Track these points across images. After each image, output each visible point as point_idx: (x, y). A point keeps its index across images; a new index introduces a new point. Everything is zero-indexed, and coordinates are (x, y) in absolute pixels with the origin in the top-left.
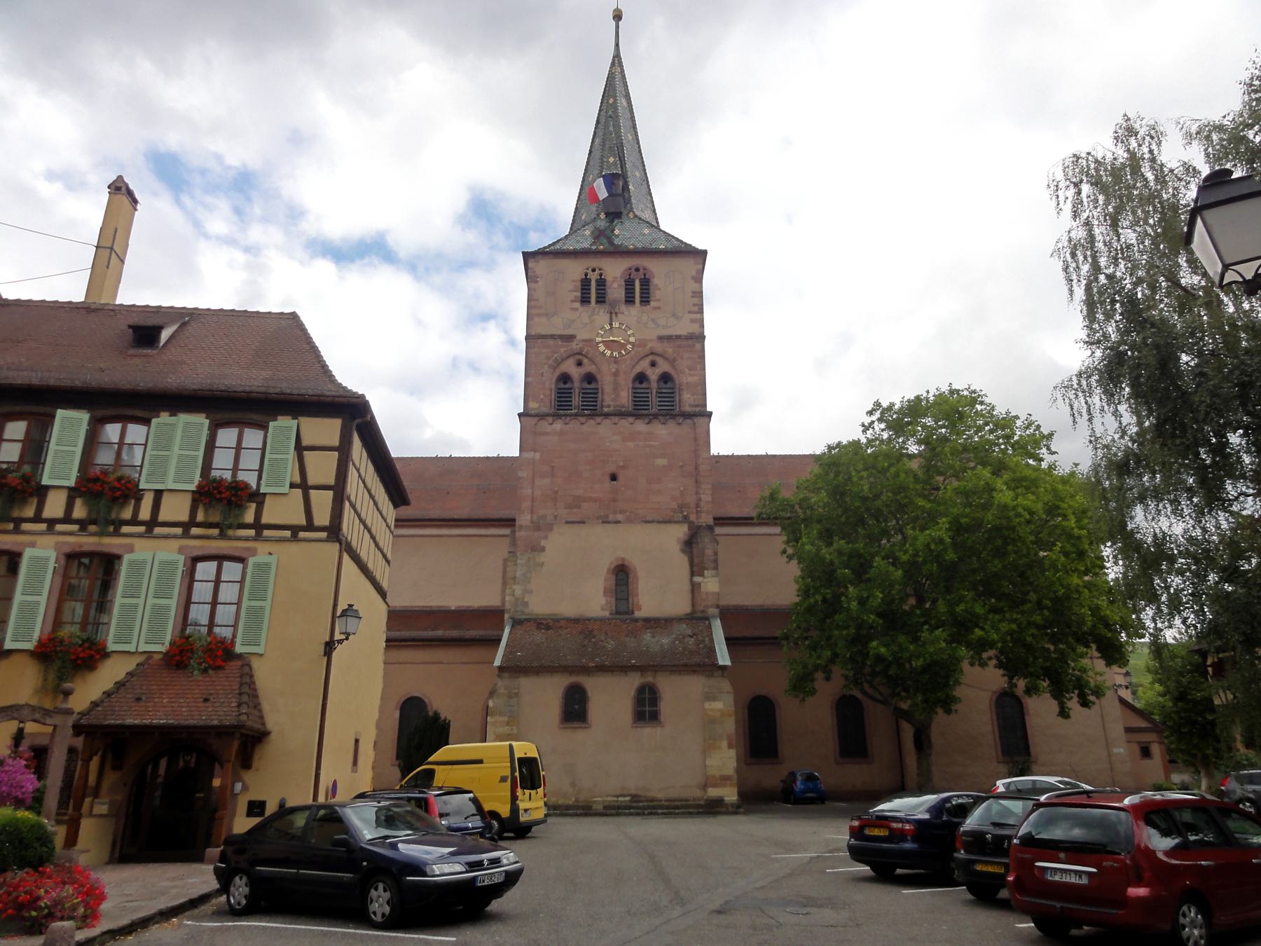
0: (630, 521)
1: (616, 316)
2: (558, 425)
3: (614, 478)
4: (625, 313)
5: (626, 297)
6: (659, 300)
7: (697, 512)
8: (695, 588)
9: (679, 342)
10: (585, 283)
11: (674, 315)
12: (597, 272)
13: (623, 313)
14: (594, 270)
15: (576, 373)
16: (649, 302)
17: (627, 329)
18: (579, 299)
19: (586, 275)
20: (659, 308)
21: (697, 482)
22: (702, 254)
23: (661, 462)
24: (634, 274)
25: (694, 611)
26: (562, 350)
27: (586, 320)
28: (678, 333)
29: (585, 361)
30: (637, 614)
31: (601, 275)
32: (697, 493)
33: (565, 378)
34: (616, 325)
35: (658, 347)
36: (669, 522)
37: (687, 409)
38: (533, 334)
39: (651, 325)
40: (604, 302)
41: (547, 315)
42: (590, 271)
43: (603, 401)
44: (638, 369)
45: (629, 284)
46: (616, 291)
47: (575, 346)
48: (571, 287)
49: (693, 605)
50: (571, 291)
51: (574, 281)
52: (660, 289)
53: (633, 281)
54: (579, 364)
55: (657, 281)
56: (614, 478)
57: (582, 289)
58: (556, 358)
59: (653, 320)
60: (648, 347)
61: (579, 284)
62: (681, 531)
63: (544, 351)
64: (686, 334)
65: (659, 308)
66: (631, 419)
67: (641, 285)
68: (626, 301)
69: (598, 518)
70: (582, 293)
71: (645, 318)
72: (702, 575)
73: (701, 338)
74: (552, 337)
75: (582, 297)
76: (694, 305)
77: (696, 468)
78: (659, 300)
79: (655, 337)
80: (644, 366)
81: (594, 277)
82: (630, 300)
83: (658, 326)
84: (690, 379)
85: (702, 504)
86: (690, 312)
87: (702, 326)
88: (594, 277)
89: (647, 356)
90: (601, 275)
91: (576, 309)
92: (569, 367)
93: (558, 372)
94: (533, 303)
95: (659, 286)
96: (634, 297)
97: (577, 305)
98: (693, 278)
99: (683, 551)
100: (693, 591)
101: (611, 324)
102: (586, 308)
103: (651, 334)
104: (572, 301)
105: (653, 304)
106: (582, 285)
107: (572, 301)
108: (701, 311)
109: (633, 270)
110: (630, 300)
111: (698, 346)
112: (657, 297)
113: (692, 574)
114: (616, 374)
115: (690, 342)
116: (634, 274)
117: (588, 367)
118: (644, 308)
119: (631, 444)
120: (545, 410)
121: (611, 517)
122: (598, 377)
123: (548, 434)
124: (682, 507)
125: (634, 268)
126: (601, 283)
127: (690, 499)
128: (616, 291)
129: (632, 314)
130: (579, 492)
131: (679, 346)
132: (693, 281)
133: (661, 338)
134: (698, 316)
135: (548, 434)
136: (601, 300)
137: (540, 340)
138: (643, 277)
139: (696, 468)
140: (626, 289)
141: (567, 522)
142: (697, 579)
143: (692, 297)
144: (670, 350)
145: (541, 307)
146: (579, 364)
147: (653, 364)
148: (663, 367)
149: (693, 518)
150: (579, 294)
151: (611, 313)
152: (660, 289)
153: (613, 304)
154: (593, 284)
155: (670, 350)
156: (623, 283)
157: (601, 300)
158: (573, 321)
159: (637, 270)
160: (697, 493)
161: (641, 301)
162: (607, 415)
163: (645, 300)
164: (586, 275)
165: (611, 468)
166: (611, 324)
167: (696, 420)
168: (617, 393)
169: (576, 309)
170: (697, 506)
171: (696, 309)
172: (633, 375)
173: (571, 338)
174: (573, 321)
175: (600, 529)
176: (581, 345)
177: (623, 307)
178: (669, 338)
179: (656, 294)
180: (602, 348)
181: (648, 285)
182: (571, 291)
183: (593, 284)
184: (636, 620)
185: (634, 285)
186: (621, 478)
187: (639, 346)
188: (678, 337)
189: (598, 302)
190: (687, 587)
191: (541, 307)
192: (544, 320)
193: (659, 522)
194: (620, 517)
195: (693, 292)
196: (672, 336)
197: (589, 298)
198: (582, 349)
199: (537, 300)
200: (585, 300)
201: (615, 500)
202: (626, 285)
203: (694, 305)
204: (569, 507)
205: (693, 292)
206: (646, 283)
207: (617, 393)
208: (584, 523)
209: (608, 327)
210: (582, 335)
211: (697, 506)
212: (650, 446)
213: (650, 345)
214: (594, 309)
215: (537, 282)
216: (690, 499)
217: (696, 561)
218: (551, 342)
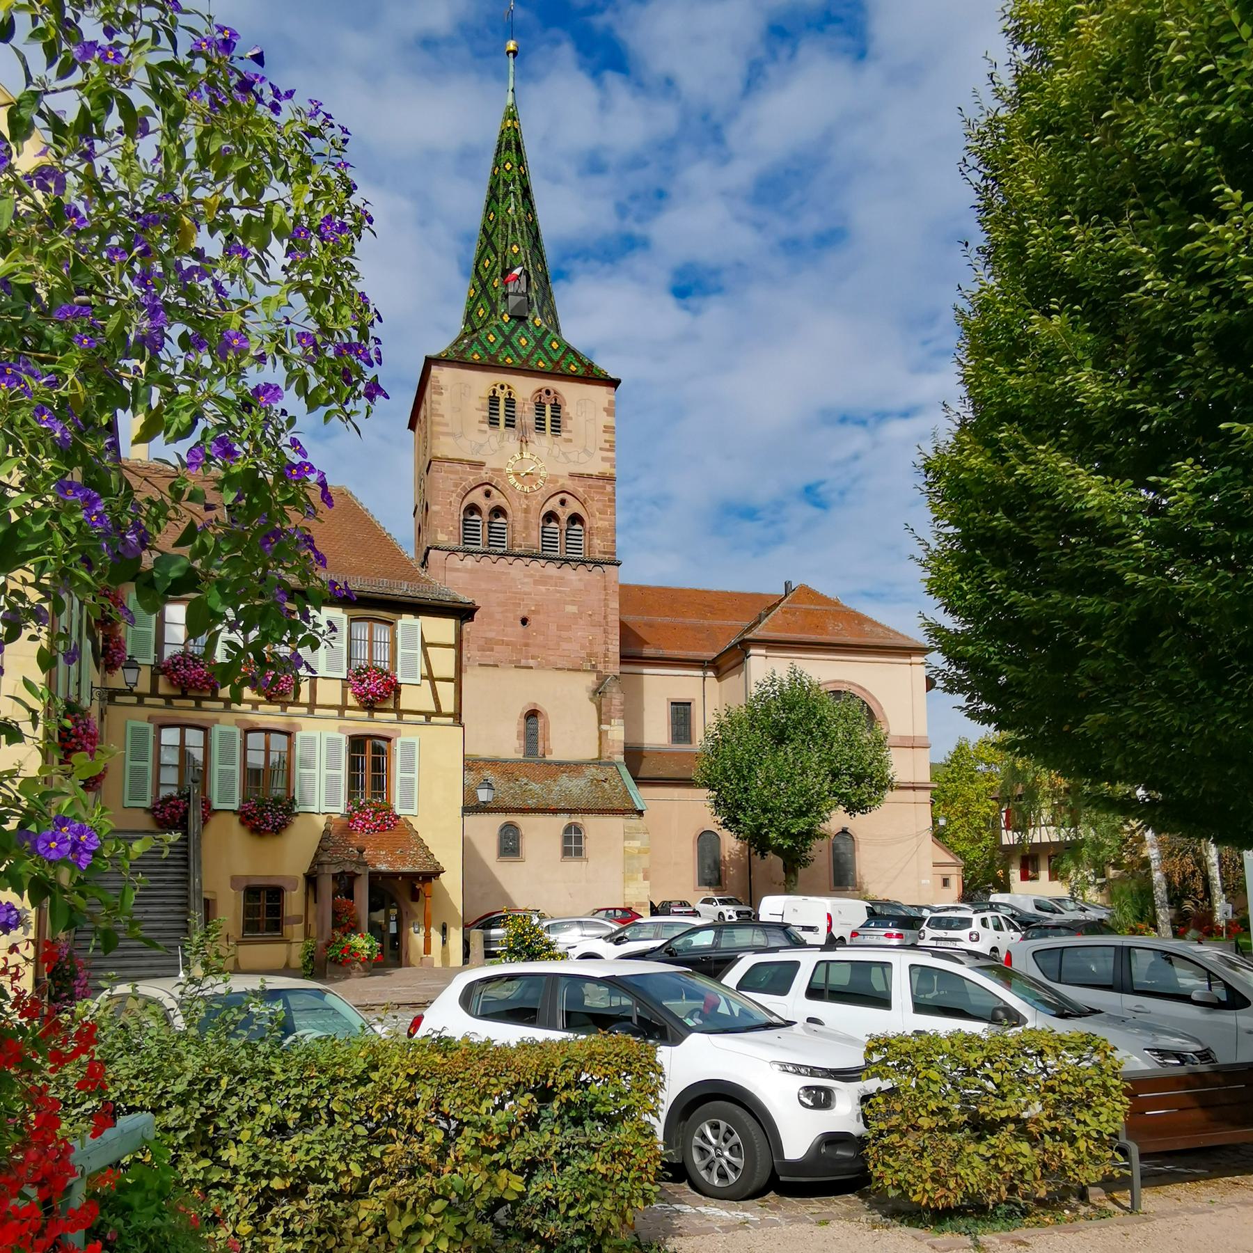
0: (541, 667)
2: (470, 561)
3: (524, 621)
6: (570, 432)
7: (605, 662)
8: (602, 735)
9: (590, 482)
10: (494, 400)
11: (585, 450)
14: (502, 387)
15: (485, 505)
18: (487, 420)
19: (494, 392)
20: (570, 441)
21: (605, 632)
23: (572, 609)
24: (545, 399)
25: (600, 757)
27: (496, 446)
29: (494, 492)
30: (548, 758)
31: (510, 394)
32: (606, 643)
33: (473, 509)
34: (526, 455)
35: (570, 485)
36: (579, 670)
37: (598, 556)
39: (562, 459)
42: (498, 388)
43: (513, 539)
44: (547, 508)
45: (540, 407)
46: (526, 414)
47: (484, 475)
48: (478, 404)
49: (600, 752)
54: (488, 494)
55: (569, 409)
56: (524, 621)
59: (564, 454)
61: (487, 402)
62: (590, 680)
63: (452, 476)
65: (570, 441)
66: (543, 562)
69: (511, 662)
71: (556, 451)
72: (609, 724)
74: (460, 461)
77: (605, 617)
78: (570, 432)
80: (553, 504)
81: (501, 395)
82: (540, 427)
84: (600, 524)
85: (610, 654)
90: (510, 394)
91: (485, 432)
92: (477, 497)
93: (465, 504)
97: (486, 427)
98: (605, 410)
99: (591, 700)
100: (600, 738)
102: (495, 432)
103: (563, 470)
105: (564, 435)
110: (540, 427)
113: (600, 722)
114: (527, 511)
115: (601, 483)
117: (498, 499)
119: (543, 588)
120: (454, 544)
121: (523, 662)
122: (509, 512)
123: (457, 570)
124: (590, 655)
126: (510, 402)
127: (600, 649)
128: (526, 414)
129: (542, 443)
130: (491, 635)
131: (590, 486)
133: (572, 475)
135: (457, 570)
139: (605, 617)
141: (481, 665)
142: (604, 727)
144: (581, 490)
145: (446, 425)
146: (488, 494)
147: (563, 502)
148: (574, 507)
149: (600, 667)
150: (487, 414)
153: (524, 428)
154: (502, 403)
155: (581, 490)
157: (510, 423)
158: (481, 446)
159: (548, 392)
160: (606, 643)
162: (519, 556)
163: (557, 427)
164: (494, 392)
165: (523, 613)
167: (605, 567)
168: (526, 533)
169: (485, 432)
170: (606, 656)
171: (607, 446)
172: (542, 514)
175: (515, 673)
177: (533, 436)
178: (581, 476)
179: (568, 425)
180: (512, 480)
183: (502, 403)
184: (549, 763)
186: (532, 622)
187: (550, 482)
188: (590, 476)
190: (597, 734)
191: (446, 425)
192: (450, 440)
193: (569, 670)
194: (531, 662)
200: (493, 422)
201: (527, 645)
204: (481, 649)
206: (556, 408)
207: (526, 533)
208: (497, 666)
209: (518, 457)
210: (492, 463)
211: (606, 656)
212: (560, 592)
213: (561, 481)
216: (600, 649)
217: (604, 709)
218: (458, 467)
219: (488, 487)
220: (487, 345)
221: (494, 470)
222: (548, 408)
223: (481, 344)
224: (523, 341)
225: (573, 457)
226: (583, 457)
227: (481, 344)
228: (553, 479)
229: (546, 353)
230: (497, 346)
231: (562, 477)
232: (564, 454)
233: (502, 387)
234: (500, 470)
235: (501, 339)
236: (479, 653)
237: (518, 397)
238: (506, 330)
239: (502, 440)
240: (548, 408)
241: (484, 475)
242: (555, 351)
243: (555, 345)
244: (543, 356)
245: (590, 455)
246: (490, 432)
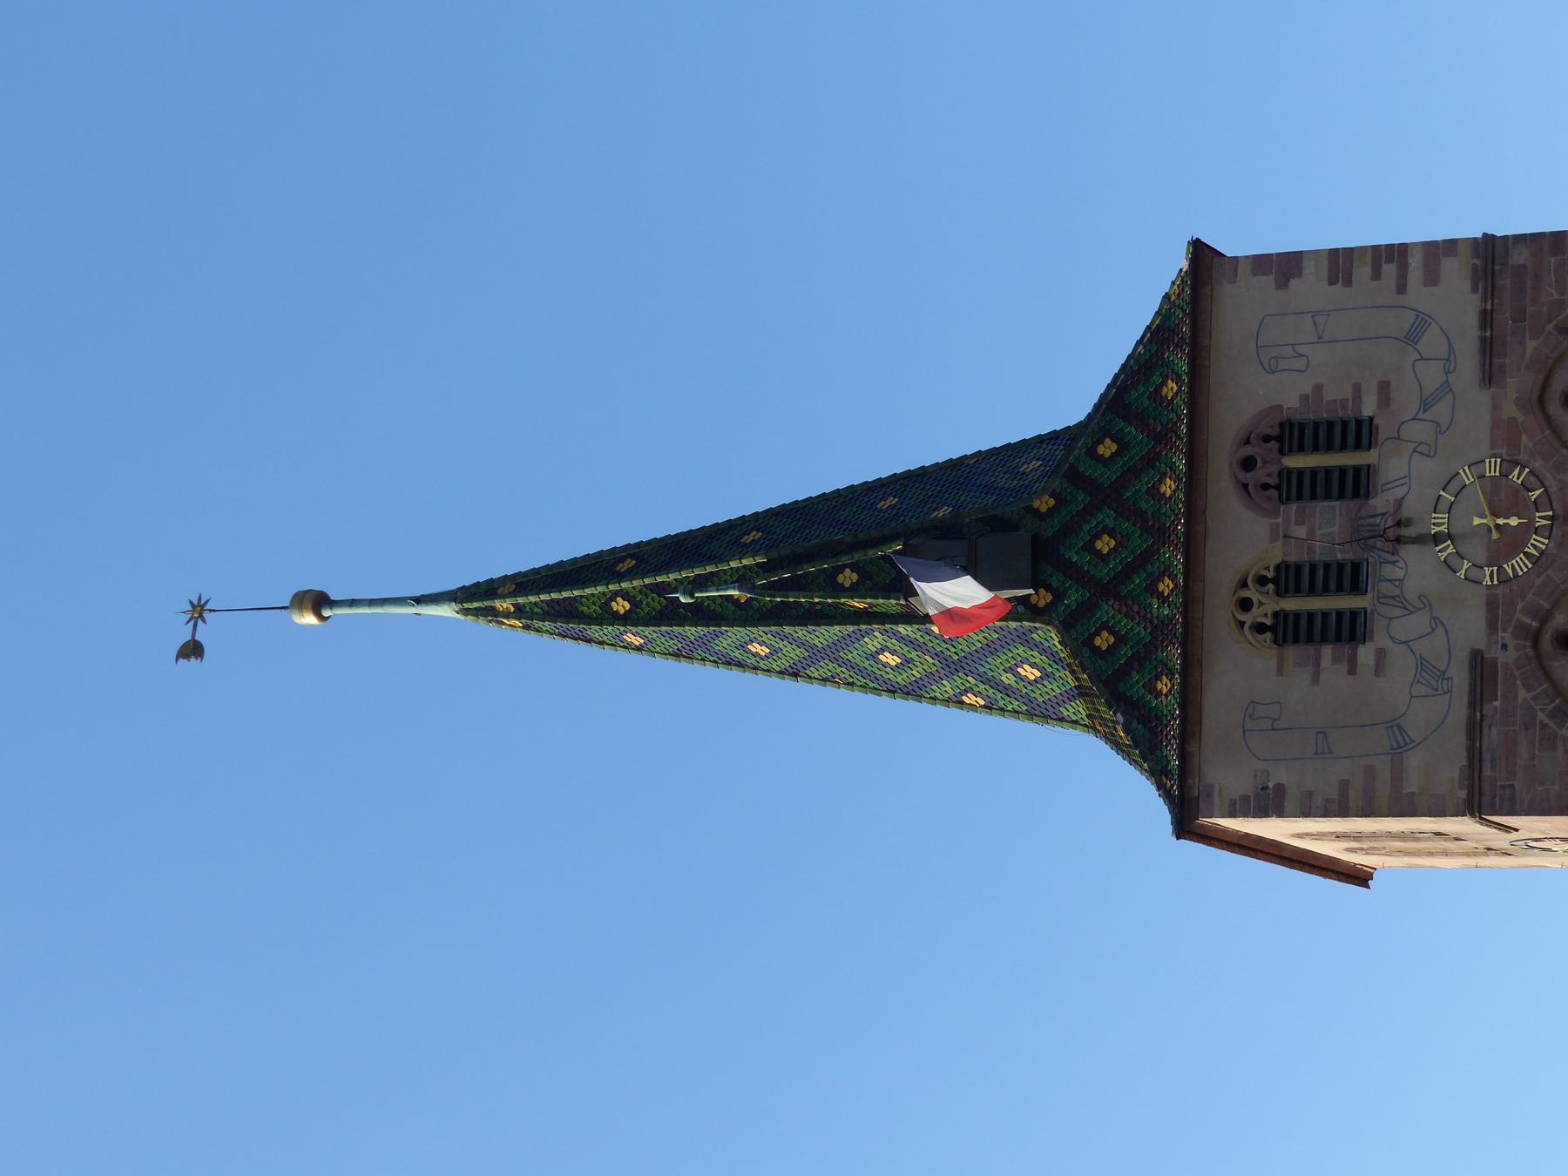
1: (1409, 522)
4: (1399, 492)
5: (1341, 496)
6: (1357, 389)
11: (1411, 338)
12: (1252, 593)
13: (1399, 503)
14: (1246, 605)
16: (1359, 423)
17: (1454, 486)
18: (1346, 649)
19: (1260, 628)
20: (1384, 389)
22: (1200, 252)
24: (1261, 474)
26: (1523, 694)
27: (1420, 621)
28: (1471, 317)
31: (1262, 581)
34: (1439, 523)
35: (1517, 384)
38: (1463, 794)
39: (1441, 410)
40: (1356, 567)
41: (1397, 754)
42: (1248, 618)
47: (1508, 655)
50: (1316, 679)
51: (1280, 671)
52: (1318, 389)
53: (1287, 473)
57: (1310, 639)
58: (1551, 715)
59: (1425, 406)
60: (1520, 417)
61: (1291, 652)
63: (1523, 753)
64: (1478, 297)
65: (1384, 389)
67: (1301, 449)
68: (1356, 495)
70: (1324, 639)
71: (1419, 431)
73: (1489, 249)
74: (1475, 729)
75: (1338, 639)
76: (1377, 275)
78: (1357, 389)
79: (1485, 397)
81: (1267, 605)
83: (1446, 387)
86: (1402, 288)
87: (1451, 246)
88: (1267, 605)
89: (1548, 419)
90: (1262, 581)
91: (1381, 654)
94: (1354, 798)
95: (1308, 390)
96: (1343, 471)
97: (1365, 653)
101: (1437, 539)
102: (1379, 625)
104: (1353, 669)
105: (1368, 409)
106: (1296, 640)
107: (1353, 669)
108: (1396, 254)
109: (1249, 477)
110: (1356, 484)
111: (1520, 257)
112: (1347, 393)
115: (1506, 283)
116: (1261, 474)
118: (1382, 435)
125: (1243, 476)
126: (1288, 578)
131: (1519, 317)
132: (1294, 282)
133: (1489, 376)
134: (1415, 262)
136: (1351, 577)
137: (1488, 772)
138: (1274, 445)
140: (1313, 497)
143: (1348, 282)
144: (1531, 345)
145: (1370, 772)
150: (1327, 651)
151: (1399, 540)
152: (1318, 389)
154: (1291, 604)
155: (1531, 345)
156: (1294, 507)
157: (1351, 577)
158: (1422, 664)
159: (1248, 464)
161: (1358, 446)
163: (1358, 433)
164: (1260, 628)
166: (1437, 539)
169: (1381, 654)
171: (1390, 270)
173: (1480, 667)
174: (1422, 664)
176: (1505, 636)
177: (1380, 502)
178: (1489, 349)
180: (1519, 564)
181: (1302, 426)
182: (1316, 679)
183: (1291, 604)
185: (1300, 472)
189: (1357, 588)
191: (1370, 772)
192: (1414, 761)
195: (1333, 281)
196: (1483, 340)
197: (1340, 614)
198: (1521, 631)
199: (1345, 785)
202: (1300, 497)
203: (1377, 275)
205: (1333, 281)
210: (1470, 629)
213: (1511, 410)
214: (1381, 597)
215: (1280, 789)
218: (1493, 735)
219: (1546, 641)
220: (1125, 651)
221: (1492, 625)
222: (1294, 462)
223: (1124, 671)
224: (1105, 544)
226: (1431, 342)
227: (1124, 671)
228: (1506, 438)
229: (1134, 472)
230: (1124, 624)
231: (1496, 407)
232: (1425, 406)
233: (1246, 605)
234: (1492, 605)
235: (1107, 611)
237: (1277, 554)
238: (1073, 597)
239: (1401, 601)
240: (1294, 462)
241: (1512, 654)
242: (1123, 447)
243: (1107, 448)
244: (1143, 484)
245: (1422, 322)
246: (1380, 639)
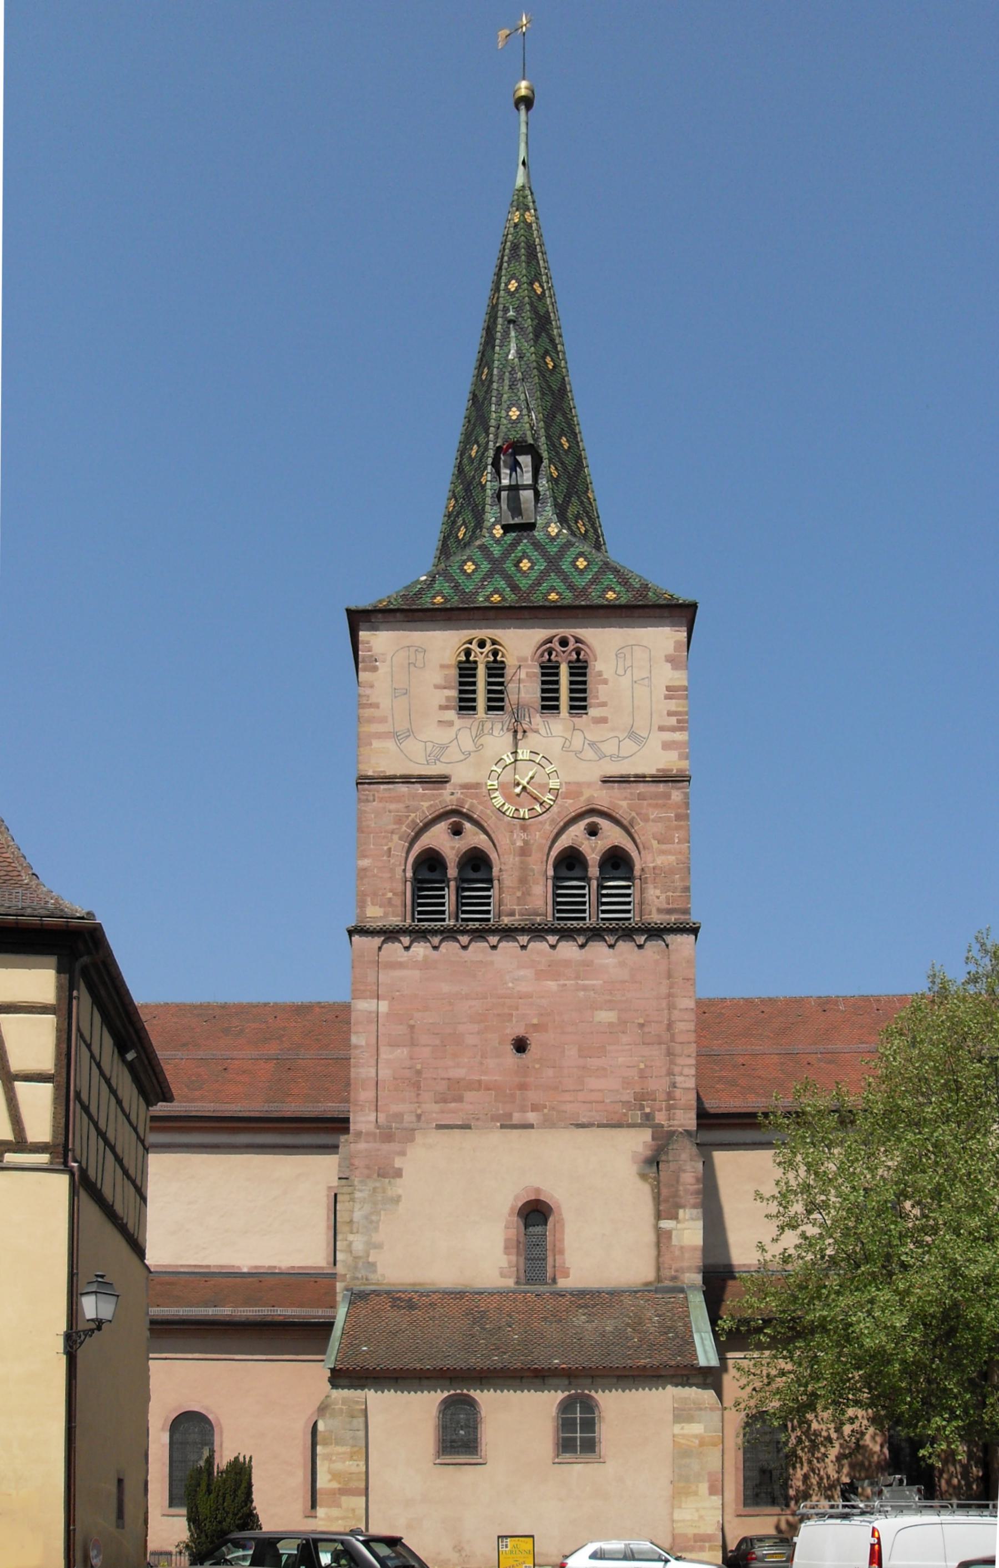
0: (549, 1124)
3: (521, 1046)
9: (642, 788)
11: (632, 735)
20: (604, 720)
23: (606, 1016)
35: (603, 798)
37: (656, 918)
39: (589, 754)
44: (564, 842)
56: (521, 1046)
59: (592, 744)
65: (604, 720)
69: (494, 1118)
71: (578, 741)
80: (576, 834)
115: (661, 787)
119: (552, 985)
121: (517, 1118)
123: (401, 965)
131: (641, 797)
133: (607, 781)
135: (401, 965)
148: (612, 836)
175: (496, 1138)
188: (640, 779)
193: (600, 1126)
194: (532, 1117)
204: (442, 1099)
208: (466, 1127)
212: (585, 988)
213: (587, 793)
225: (609, 748)
226: (629, 746)
228: (573, 790)
231: (589, 785)
232: (592, 744)
236: (437, 1107)
